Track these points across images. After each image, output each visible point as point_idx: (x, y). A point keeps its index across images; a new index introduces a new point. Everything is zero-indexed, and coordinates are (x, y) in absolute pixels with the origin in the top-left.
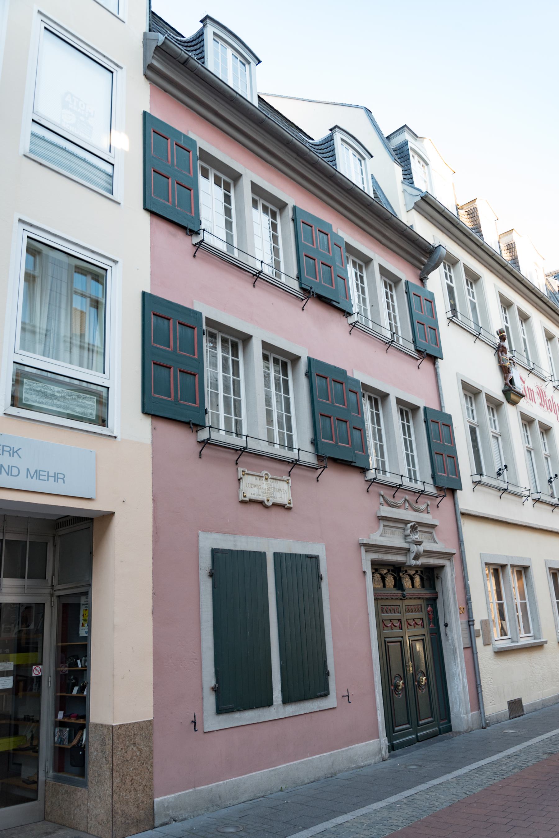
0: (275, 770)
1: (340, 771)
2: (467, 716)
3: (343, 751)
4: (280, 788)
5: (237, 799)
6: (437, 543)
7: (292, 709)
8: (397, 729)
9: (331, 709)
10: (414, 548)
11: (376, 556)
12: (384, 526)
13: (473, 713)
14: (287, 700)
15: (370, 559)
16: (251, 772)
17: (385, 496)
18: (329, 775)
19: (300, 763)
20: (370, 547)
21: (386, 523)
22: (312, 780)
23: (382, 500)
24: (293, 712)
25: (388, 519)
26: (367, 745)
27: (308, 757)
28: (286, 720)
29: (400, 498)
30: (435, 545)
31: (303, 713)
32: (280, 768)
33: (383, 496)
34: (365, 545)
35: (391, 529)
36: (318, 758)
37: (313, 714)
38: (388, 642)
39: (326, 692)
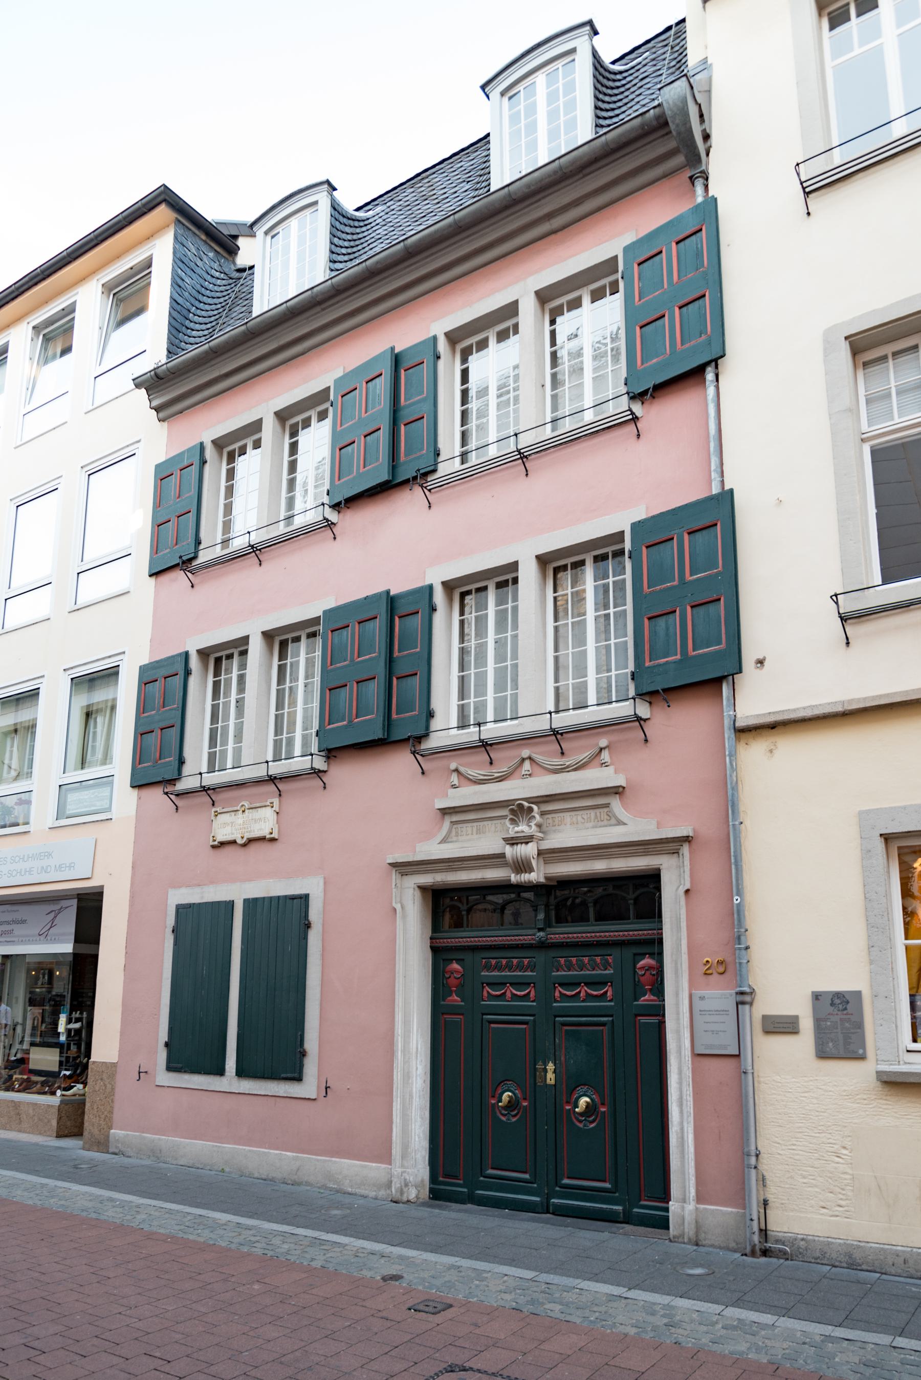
0: (219, 1147)
1: (308, 1184)
2: (683, 1208)
3: (318, 1160)
4: (221, 1168)
5: (176, 1159)
6: (625, 824)
7: (248, 1086)
8: (491, 1172)
9: (305, 1099)
10: (509, 851)
11: (427, 879)
12: (451, 822)
13: (702, 1206)
14: (241, 1073)
15: (413, 886)
16: (196, 1139)
17: (462, 769)
18: (289, 1182)
19: (250, 1151)
20: (404, 868)
21: (455, 818)
22: (263, 1177)
23: (455, 779)
24: (249, 1089)
25: (457, 810)
26: (362, 1166)
27: (266, 1148)
28: (240, 1096)
29: (505, 759)
30: (620, 829)
31: (263, 1094)
32: (224, 1147)
33: (456, 770)
34: (394, 865)
35: (475, 824)
36: (277, 1154)
37: (278, 1099)
38: (491, 1022)
39: (296, 1075)
